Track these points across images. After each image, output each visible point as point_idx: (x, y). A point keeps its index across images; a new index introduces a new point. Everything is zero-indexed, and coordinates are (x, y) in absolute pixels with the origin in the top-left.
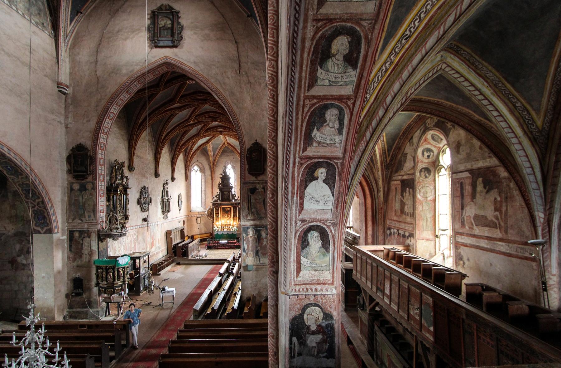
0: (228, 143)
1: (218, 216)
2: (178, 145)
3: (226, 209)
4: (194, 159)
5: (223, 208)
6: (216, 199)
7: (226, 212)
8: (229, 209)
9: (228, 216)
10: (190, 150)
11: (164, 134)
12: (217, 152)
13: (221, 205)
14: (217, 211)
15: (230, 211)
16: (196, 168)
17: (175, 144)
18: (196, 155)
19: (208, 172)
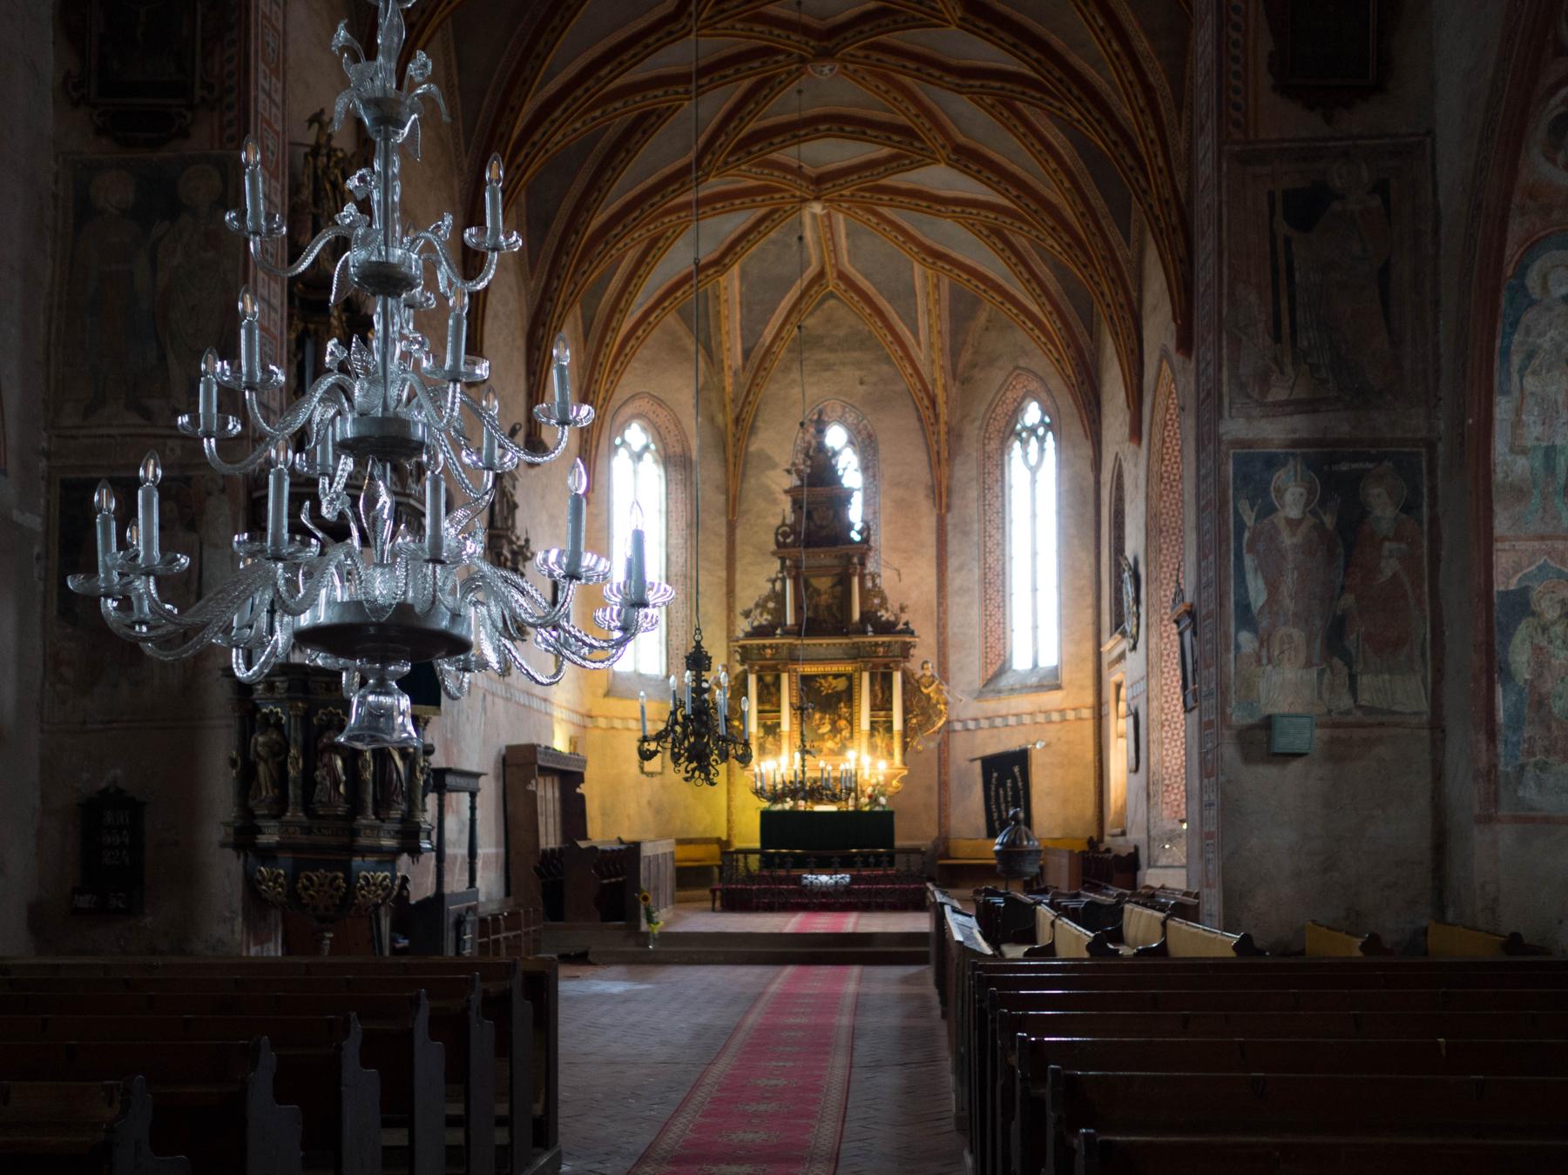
0: (842, 276)
1: (771, 729)
2: (572, 226)
3: (827, 686)
4: (629, 382)
5: (807, 680)
6: (765, 619)
7: (824, 702)
8: (841, 684)
9: (835, 730)
10: (614, 308)
11: (529, 109)
12: (769, 333)
13: (794, 659)
14: (769, 694)
15: (849, 696)
16: (636, 435)
17: (558, 227)
18: (643, 353)
19: (710, 472)
